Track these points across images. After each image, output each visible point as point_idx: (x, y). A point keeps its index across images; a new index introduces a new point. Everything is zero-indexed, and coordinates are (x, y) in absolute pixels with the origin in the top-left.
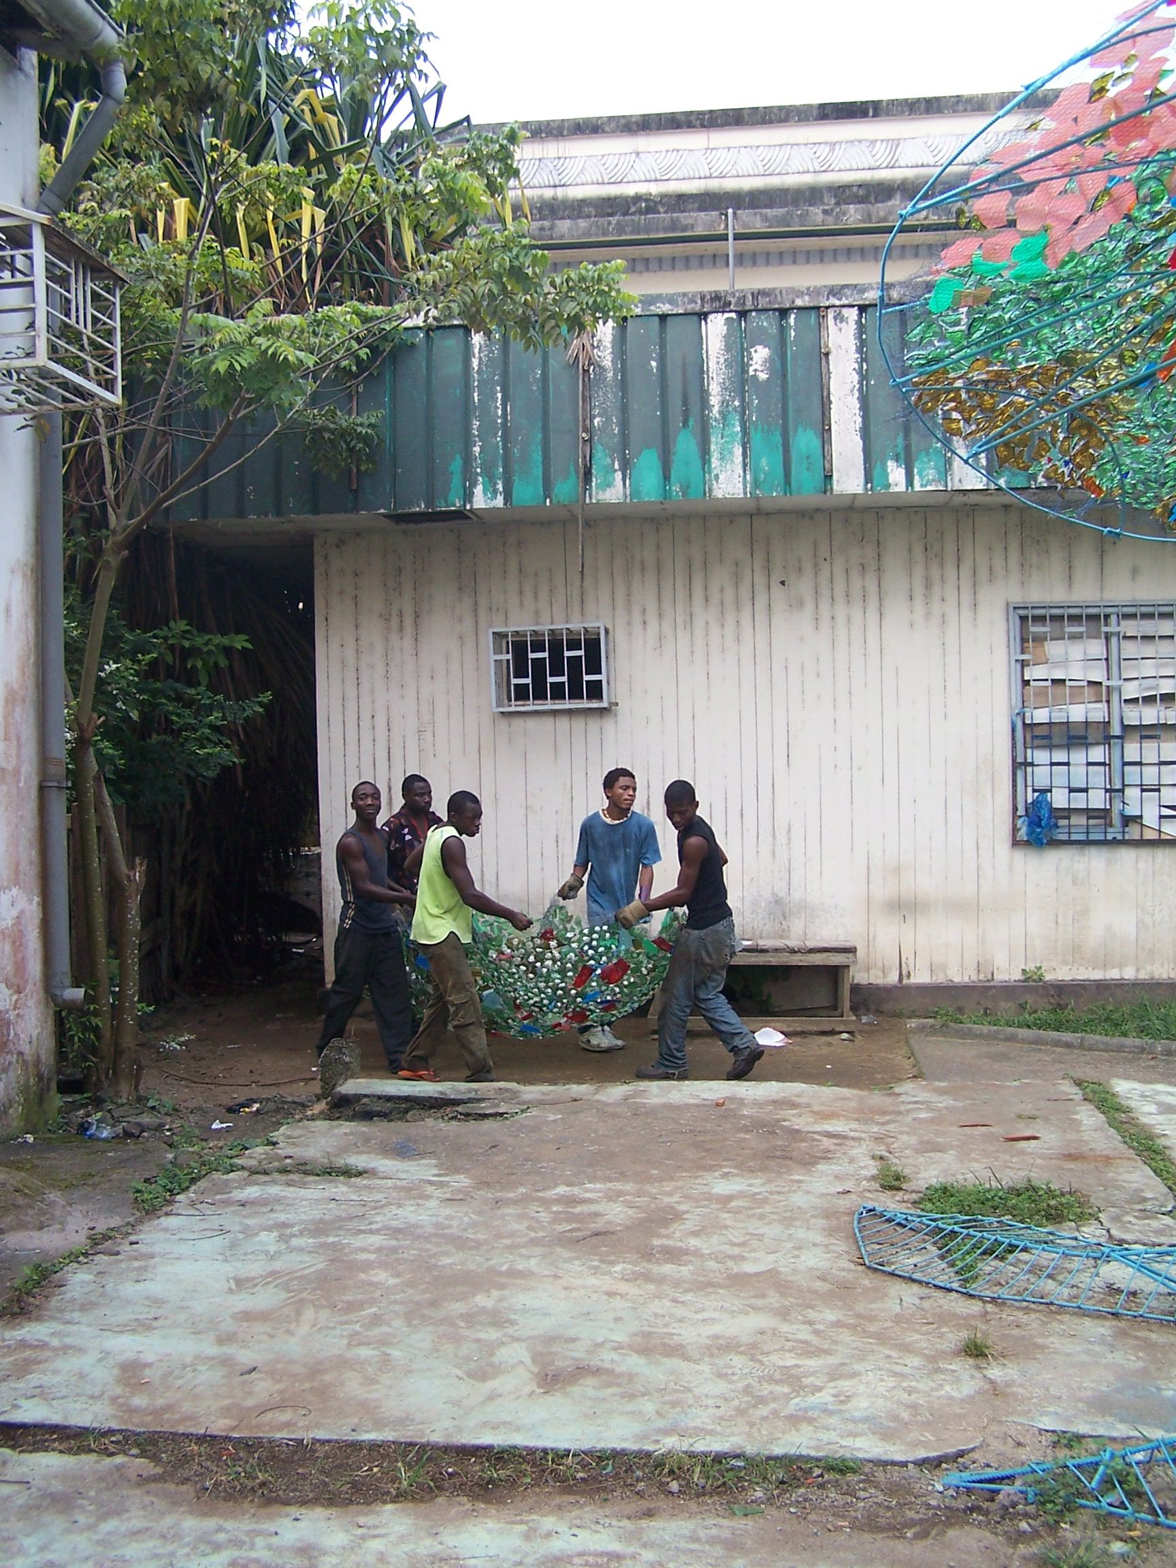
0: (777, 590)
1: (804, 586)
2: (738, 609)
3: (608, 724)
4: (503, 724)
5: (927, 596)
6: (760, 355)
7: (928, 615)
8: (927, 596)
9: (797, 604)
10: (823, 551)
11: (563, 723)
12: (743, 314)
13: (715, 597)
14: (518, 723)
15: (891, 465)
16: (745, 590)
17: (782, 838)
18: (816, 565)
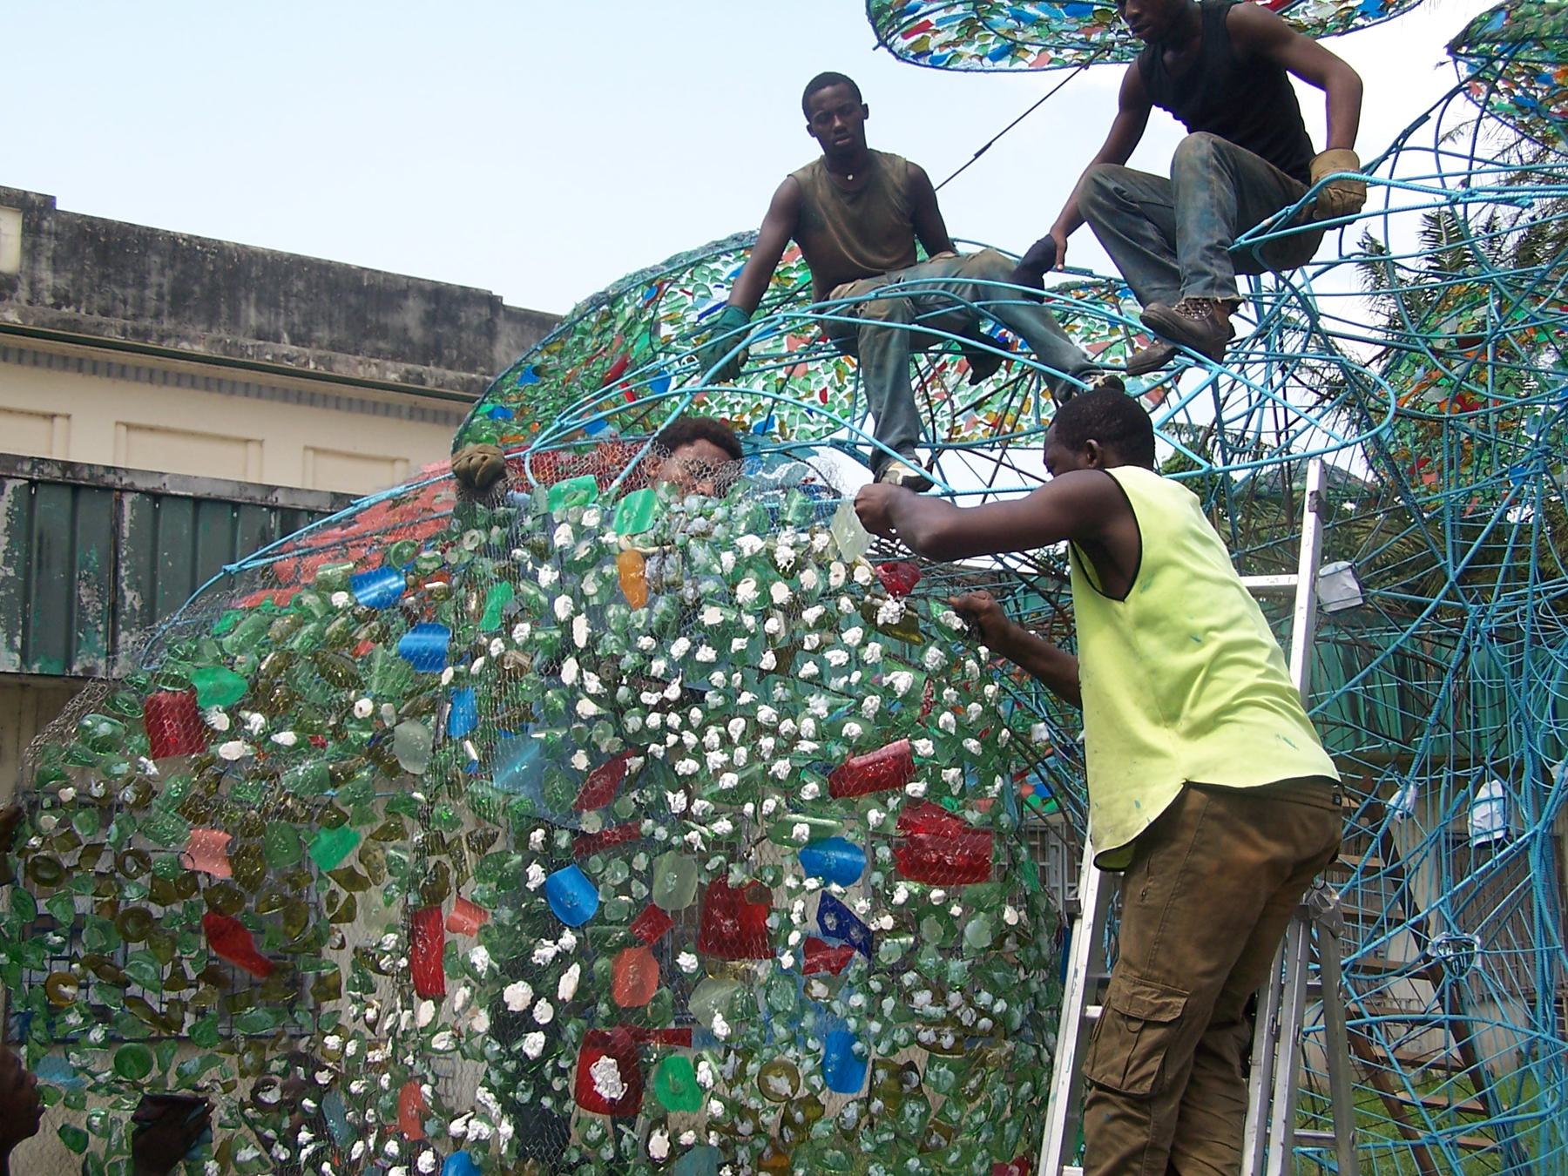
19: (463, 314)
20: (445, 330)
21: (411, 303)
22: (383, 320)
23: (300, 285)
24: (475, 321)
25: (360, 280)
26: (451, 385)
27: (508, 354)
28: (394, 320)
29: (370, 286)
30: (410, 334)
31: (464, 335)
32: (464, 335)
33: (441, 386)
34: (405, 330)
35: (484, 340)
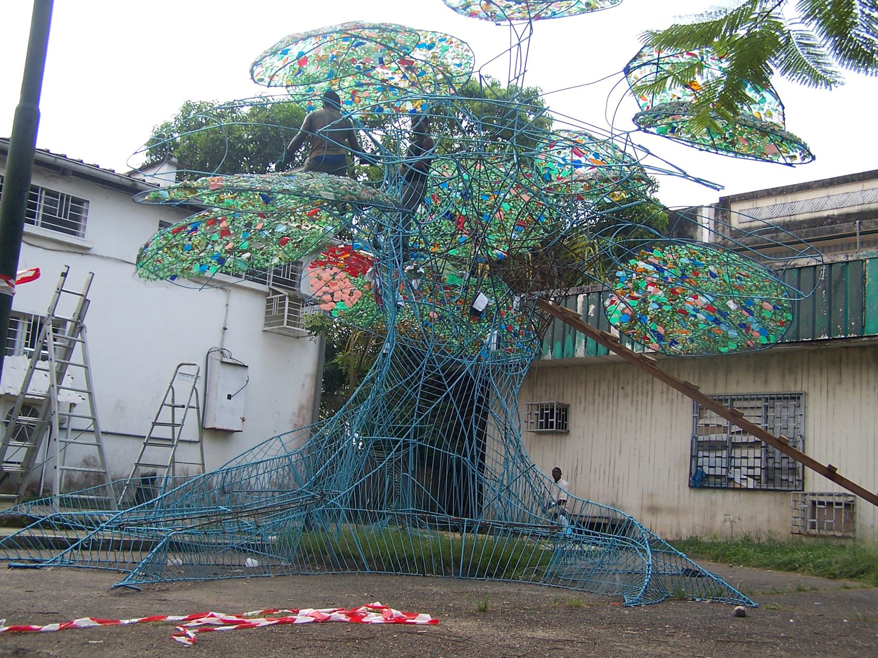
0: (621, 392)
1: (629, 389)
2: (608, 397)
3: (568, 438)
4: (538, 437)
5: (667, 393)
6: (592, 307)
7: (667, 400)
8: (667, 393)
9: (626, 396)
10: (635, 377)
11: (555, 437)
12: (588, 294)
13: (602, 393)
14: (543, 437)
15: (627, 344)
16: (611, 390)
17: (616, 482)
18: (633, 382)
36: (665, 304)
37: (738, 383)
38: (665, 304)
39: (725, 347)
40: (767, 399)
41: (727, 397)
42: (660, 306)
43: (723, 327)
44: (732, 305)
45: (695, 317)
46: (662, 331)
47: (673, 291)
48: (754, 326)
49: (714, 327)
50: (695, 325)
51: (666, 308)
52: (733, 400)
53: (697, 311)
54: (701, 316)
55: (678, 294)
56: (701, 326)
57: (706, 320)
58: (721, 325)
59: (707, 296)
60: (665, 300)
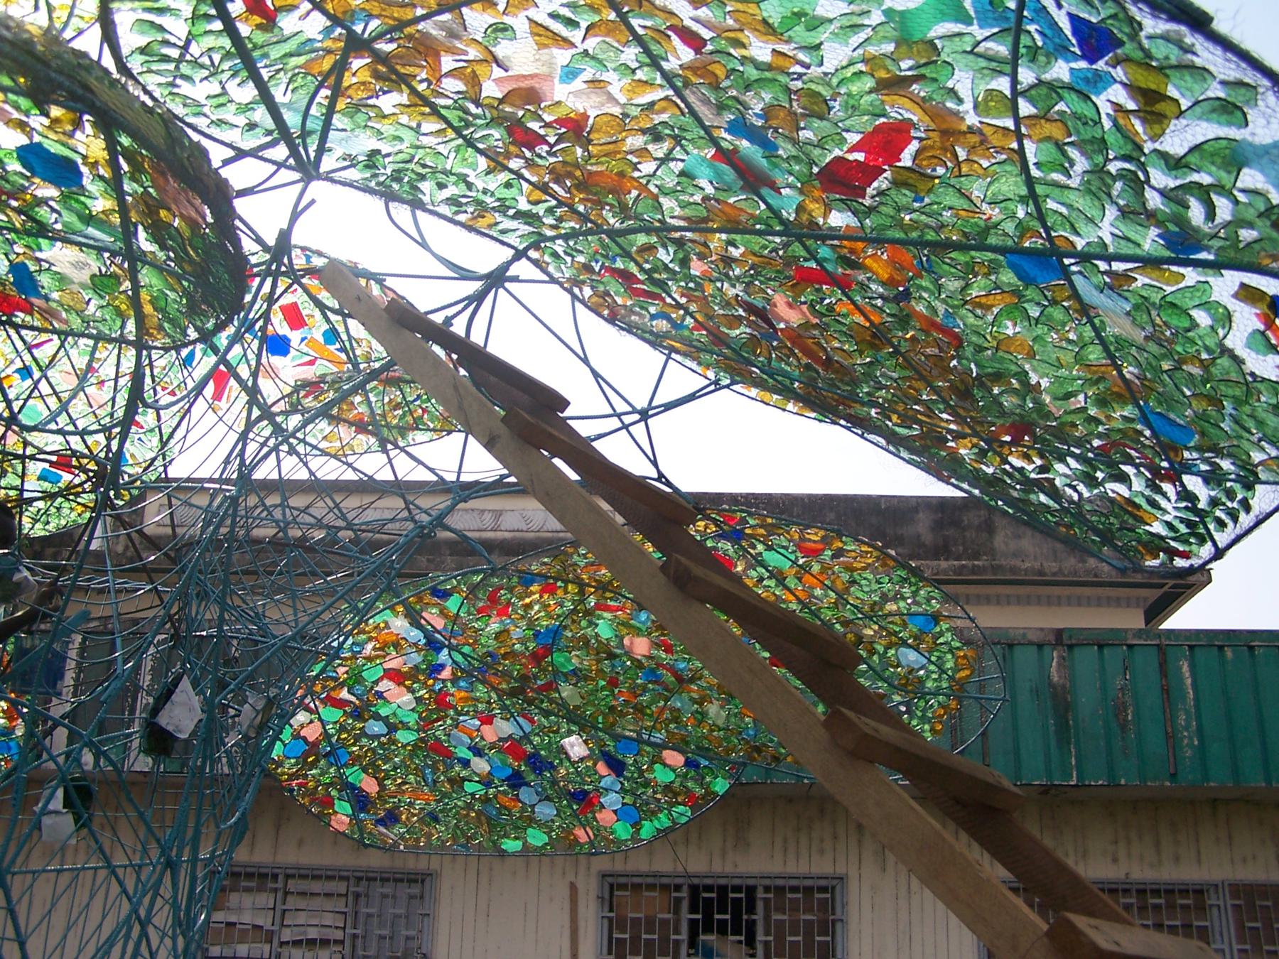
19: (965, 518)
20: (951, 532)
21: (921, 515)
22: (900, 532)
23: (832, 516)
24: (976, 522)
25: (879, 505)
26: (945, 572)
27: (1006, 544)
28: (908, 531)
29: (887, 509)
30: (923, 538)
31: (967, 534)
32: (967, 534)
33: (937, 574)
34: (919, 536)
35: (985, 535)
36: (405, 726)
37: (301, 843)
38: (405, 726)
39: (516, 838)
40: (359, 879)
41: (276, 871)
42: (392, 728)
43: (526, 795)
44: (575, 746)
45: (466, 763)
46: (370, 786)
47: (441, 700)
48: (611, 800)
49: (504, 793)
50: (458, 782)
51: (404, 737)
52: (288, 877)
53: (478, 752)
54: (481, 765)
55: (450, 706)
56: (469, 787)
57: (490, 773)
58: (523, 789)
59: (520, 719)
60: (412, 719)
